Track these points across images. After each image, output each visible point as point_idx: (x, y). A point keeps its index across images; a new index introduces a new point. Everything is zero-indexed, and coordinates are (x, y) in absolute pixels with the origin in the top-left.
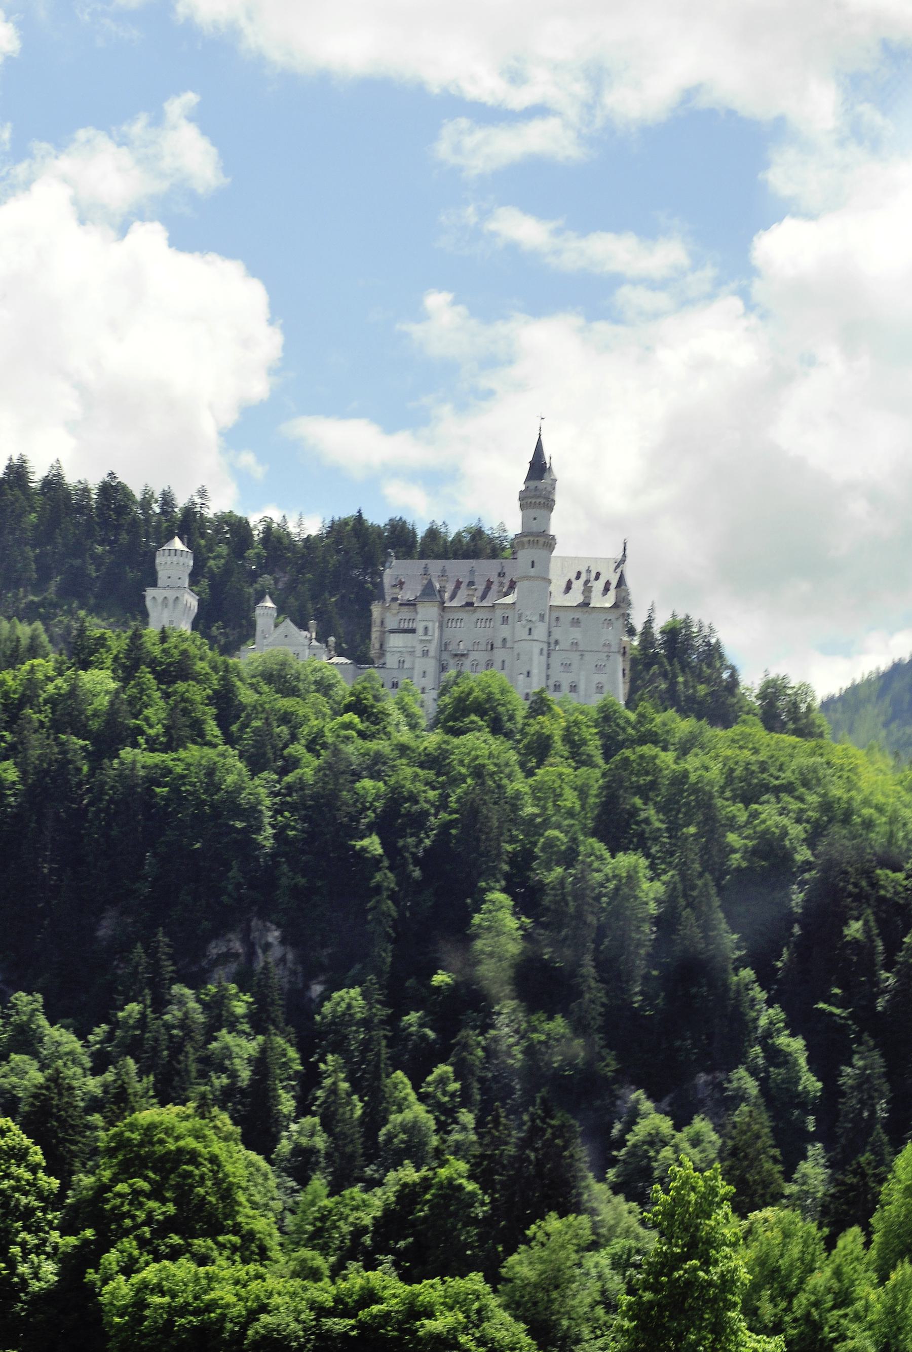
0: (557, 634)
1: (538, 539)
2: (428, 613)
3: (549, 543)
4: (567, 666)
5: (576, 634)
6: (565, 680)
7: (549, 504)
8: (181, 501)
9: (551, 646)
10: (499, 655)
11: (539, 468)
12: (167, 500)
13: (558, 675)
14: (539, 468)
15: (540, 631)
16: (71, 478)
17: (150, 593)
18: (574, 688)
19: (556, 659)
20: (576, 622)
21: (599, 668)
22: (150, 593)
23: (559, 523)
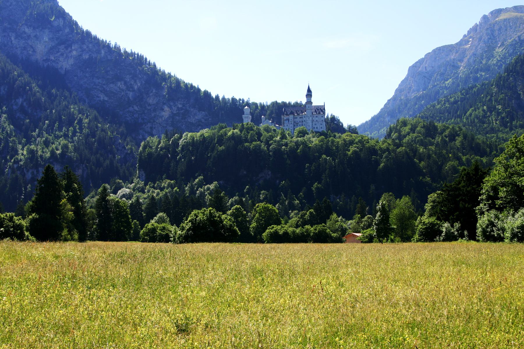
0: (314, 119)
1: (309, 102)
2: (291, 117)
3: (311, 103)
4: (315, 124)
5: (317, 119)
6: (315, 126)
7: (311, 96)
8: (246, 100)
9: (313, 121)
10: (304, 123)
11: (309, 91)
12: (243, 100)
13: (314, 126)
14: (309, 91)
15: (311, 118)
16: (226, 97)
17: (243, 116)
18: (317, 128)
19: (314, 123)
20: (317, 117)
21: (321, 124)
22: (243, 116)
23: (313, 100)
